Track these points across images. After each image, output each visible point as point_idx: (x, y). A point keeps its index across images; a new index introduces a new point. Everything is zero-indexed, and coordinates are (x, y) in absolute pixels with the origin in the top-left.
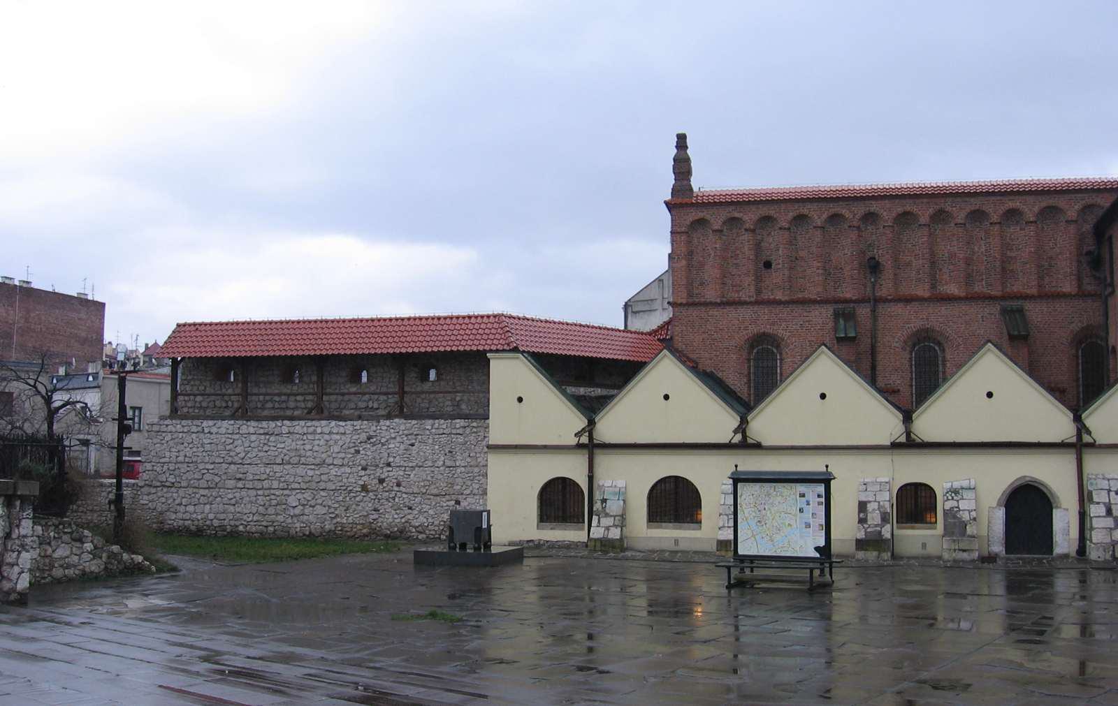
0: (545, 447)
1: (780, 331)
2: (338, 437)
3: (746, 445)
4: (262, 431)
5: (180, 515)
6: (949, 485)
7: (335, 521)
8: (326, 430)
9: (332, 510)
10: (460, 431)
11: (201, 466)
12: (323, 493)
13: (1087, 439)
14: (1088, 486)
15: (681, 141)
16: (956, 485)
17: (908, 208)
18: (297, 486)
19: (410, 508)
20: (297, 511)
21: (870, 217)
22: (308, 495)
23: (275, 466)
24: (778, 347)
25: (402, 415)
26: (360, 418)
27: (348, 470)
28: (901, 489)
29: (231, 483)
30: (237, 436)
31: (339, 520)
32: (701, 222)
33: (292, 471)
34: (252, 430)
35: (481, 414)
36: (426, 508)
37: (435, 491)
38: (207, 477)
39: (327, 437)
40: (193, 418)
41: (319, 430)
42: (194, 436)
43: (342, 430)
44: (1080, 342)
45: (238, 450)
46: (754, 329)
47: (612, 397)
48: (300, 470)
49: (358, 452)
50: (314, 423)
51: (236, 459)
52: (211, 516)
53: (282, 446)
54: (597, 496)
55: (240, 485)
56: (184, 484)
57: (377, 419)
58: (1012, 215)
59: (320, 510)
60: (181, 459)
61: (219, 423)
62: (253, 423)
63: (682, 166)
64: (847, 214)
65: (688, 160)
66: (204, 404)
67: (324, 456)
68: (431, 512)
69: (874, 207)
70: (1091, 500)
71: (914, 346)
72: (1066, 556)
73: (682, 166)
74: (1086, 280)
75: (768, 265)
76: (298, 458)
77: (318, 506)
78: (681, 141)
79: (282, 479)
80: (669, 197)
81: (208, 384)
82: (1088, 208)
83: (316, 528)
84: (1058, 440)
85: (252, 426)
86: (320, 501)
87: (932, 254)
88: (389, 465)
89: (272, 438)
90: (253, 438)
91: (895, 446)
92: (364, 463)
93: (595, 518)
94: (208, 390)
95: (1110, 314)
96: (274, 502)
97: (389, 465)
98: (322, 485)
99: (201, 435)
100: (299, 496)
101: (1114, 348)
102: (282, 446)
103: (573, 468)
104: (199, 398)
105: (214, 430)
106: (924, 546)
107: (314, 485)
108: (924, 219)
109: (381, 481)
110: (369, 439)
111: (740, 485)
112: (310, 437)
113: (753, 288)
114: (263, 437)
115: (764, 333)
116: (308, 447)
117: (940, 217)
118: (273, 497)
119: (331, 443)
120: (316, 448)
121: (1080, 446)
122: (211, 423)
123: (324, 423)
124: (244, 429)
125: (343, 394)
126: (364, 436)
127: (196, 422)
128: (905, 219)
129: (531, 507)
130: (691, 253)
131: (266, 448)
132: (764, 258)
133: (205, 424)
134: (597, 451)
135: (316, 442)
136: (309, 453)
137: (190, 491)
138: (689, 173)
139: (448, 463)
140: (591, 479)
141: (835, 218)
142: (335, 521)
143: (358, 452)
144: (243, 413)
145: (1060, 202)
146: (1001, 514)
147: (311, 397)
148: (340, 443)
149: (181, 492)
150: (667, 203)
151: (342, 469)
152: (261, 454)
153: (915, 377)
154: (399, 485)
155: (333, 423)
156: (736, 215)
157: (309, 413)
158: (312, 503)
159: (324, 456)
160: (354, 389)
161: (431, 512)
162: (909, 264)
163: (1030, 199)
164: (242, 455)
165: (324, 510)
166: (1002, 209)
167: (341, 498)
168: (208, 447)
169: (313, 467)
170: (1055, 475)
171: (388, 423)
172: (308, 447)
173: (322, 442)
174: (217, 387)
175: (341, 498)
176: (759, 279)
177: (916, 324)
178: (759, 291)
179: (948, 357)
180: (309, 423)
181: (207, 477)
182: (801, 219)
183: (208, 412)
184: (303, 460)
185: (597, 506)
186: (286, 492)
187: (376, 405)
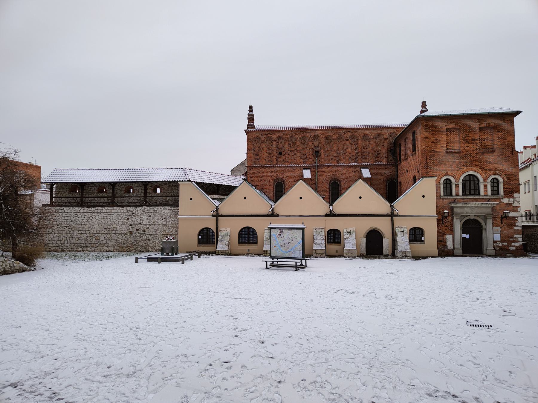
0: (200, 216)
1: (284, 176)
3: (273, 214)
6: (345, 230)
10: (168, 211)
13: (395, 213)
14: (397, 230)
15: (251, 108)
16: (348, 230)
17: (329, 134)
18: (103, 232)
19: (149, 240)
20: (104, 242)
21: (316, 137)
22: (108, 236)
24: (284, 182)
25: (145, 205)
26: (129, 206)
27: (124, 226)
28: (328, 231)
29: (76, 232)
32: (257, 138)
34: (85, 211)
35: (176, 204)
36: (155, 239)
37: (159, 234)
40: (62, 206)
42: (60, 214)
43: (122, 211)
44: (388, 180)
46: (275, 176)
47: (224, 199)
49: (128, 219)
50: (112, 208)
51: (78, 222)
54: (220, 234)
55: (80, 232)
56: (57, 232)
57: (137, 206)
58: (365, 137)
59: (113, 241)
61: (71, 208)
63: (251, 118)
64: (308, 136)
65: (253, 115)
66: (65, 201)
67: (115, 221)
68: (157, 241)
69: (318, 133)
70: (396, 235)
71: (330, 181)
72: (388, 255)
73: (251, 118)
74: (390, 159)
75: (280, 153)
78: (251, 108)
80: (246, 128)
81: (67, 193)
82: (392, 134)
84: (385, 213)
85: (85, 209)
86: (113, 238)
87: (338, 150)
88: (140, 224)
89: (94, 214)
90: (86, 214)
91: (326, 215)
92: (131, 223)
93: (219, 242)
94: (67, 196)
95: (399, 171)
96: (94, 239)
97: (140, 224)
99: (64, 214)
100: (105, 236)
101: (400, 183)
103: (211, 224)
104: (63, 199)
105: (69, 211)
106: (337, 251)
108: (335, 137)
109: (138, 230)
110: (133, 213)
111: (272, 230)
113: (275, 161)
115: (279, 177)
117: (340, 137)
120: (112, 218)
121: (392, 215)
122: (68, 208)
123: (115, 208)
125: (123, 197)
126: (131, 213)
127: (62, 208)
128: (328, 139)
129: (195, 238)
130: (254, 149)
132: (279, 151)
133: (65, 209)
134: (219, 218)
136: (109, 220)
137: (58, 235)
138: (253, 120)
139: (165, 223)
140: (217, 228)
141: (304, 137)
143: (128, 219)
144: (81, 204)
145: (383, 132)
146: (364, 240)
147: (110, 198)
149: (55, 236)
150: (245, 131)
153: (334, 192)
154: (144, 231)
155: (119, 208)
156: (270, 135)
157: (109, 204)
158: (110, 239)
160: (127, 195)
161: (157, 241)
162: (329, 153)
163: (372, 131)
164: (81, 221)
166: (362, 135)
168: (66, 218)
170: (383, 225)
171: (140, 208)
172: (108, 217)
174: (71, 195)
176: (277, 159)
177: (331, 174)
178: (277, 163)
179: (342, 185)
180: (109, 208)
181: (66, 229)
182: (292, 137)
183: (68, 204)
184: (106, 222)
185: (220, 238)
187: (136, 201)
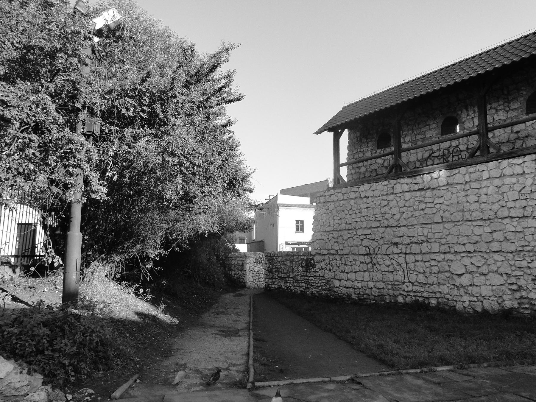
2: (514, 180)
4: (416, 187)
5: (343, 283)
7: (518, 295)
8: (496, 173)
9: (513, 280)
11: (359, 232)
12: (496, 257)
22: (477, 260)
23: (433, 226)
30: (391, 197)
31: (524, 293)
33: (454, 230)
34: (406, 188)
38: (366, 243)
39: (497, 182)
41: (485, 175)
42: (352, 202)
43: (518, 170)
45: (394, 211)
48: (465, 228)
51: (393, 222)
52: (371, 284)
53: (441, 200)
59: (497, 280)
60: (343, 226)
61: (374, 186)
62: (407, 180)
67: (495, 207)
76: (460, 214)
77: (491, 274)
79: (443, 241)
83: (491, 305)
86: (494, 268)
89: (429, 194)
90: (408, 195)
98: (495, 246)
99: (359, 201)
100: (467, 261)
102: (441, 200)
107: (483, 247)
112: (474, 185)
114: (418, 193)
116: (473, 198)
118: (433, 263)
119: (505, 189)
120: (484, 198)
122: (366, 187)
124: (398, 188)
131: (423, 206)
135: (484, 190)
142: (518, 295)
148: (518, 187)
151: (524, 223)
152: (417, 213)
155: (505, 163)
157: (472, 155)
158: (484, 269)
159: (495, 207)
164: (397, 217)
165: (501, 280)
167: (524, 264)
169: (481, 223)
173: (491, 190)
175: (524, 264)
180: (472, 169)
184: (467, 216)
186: (448, 256)
